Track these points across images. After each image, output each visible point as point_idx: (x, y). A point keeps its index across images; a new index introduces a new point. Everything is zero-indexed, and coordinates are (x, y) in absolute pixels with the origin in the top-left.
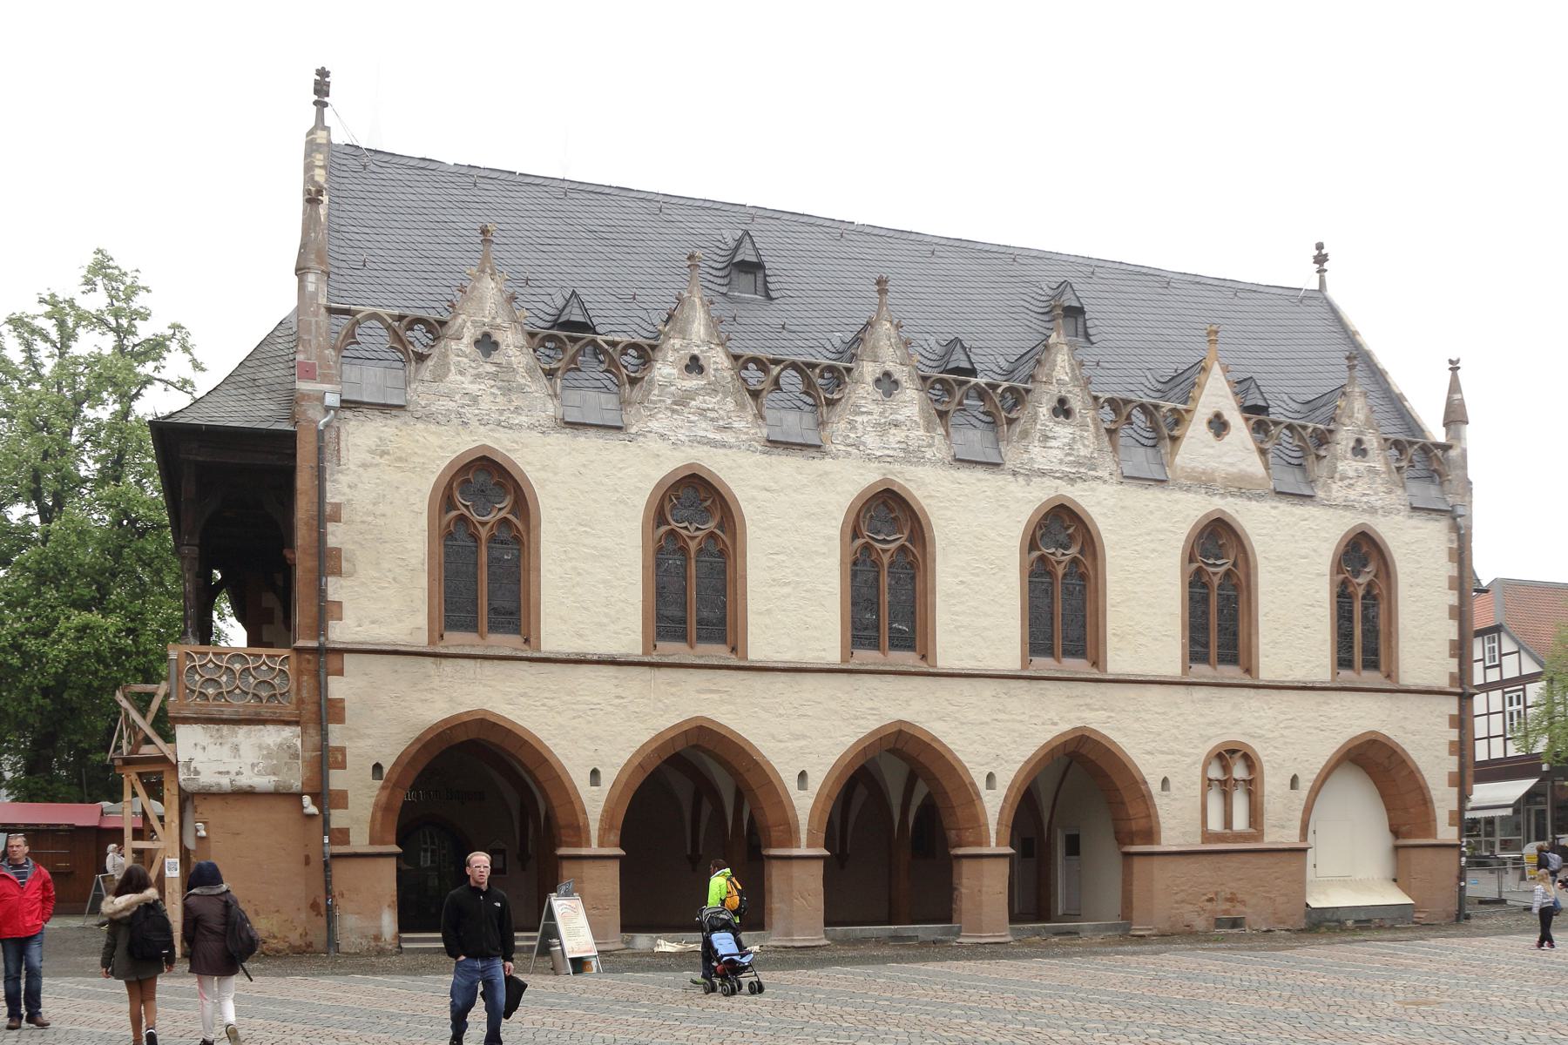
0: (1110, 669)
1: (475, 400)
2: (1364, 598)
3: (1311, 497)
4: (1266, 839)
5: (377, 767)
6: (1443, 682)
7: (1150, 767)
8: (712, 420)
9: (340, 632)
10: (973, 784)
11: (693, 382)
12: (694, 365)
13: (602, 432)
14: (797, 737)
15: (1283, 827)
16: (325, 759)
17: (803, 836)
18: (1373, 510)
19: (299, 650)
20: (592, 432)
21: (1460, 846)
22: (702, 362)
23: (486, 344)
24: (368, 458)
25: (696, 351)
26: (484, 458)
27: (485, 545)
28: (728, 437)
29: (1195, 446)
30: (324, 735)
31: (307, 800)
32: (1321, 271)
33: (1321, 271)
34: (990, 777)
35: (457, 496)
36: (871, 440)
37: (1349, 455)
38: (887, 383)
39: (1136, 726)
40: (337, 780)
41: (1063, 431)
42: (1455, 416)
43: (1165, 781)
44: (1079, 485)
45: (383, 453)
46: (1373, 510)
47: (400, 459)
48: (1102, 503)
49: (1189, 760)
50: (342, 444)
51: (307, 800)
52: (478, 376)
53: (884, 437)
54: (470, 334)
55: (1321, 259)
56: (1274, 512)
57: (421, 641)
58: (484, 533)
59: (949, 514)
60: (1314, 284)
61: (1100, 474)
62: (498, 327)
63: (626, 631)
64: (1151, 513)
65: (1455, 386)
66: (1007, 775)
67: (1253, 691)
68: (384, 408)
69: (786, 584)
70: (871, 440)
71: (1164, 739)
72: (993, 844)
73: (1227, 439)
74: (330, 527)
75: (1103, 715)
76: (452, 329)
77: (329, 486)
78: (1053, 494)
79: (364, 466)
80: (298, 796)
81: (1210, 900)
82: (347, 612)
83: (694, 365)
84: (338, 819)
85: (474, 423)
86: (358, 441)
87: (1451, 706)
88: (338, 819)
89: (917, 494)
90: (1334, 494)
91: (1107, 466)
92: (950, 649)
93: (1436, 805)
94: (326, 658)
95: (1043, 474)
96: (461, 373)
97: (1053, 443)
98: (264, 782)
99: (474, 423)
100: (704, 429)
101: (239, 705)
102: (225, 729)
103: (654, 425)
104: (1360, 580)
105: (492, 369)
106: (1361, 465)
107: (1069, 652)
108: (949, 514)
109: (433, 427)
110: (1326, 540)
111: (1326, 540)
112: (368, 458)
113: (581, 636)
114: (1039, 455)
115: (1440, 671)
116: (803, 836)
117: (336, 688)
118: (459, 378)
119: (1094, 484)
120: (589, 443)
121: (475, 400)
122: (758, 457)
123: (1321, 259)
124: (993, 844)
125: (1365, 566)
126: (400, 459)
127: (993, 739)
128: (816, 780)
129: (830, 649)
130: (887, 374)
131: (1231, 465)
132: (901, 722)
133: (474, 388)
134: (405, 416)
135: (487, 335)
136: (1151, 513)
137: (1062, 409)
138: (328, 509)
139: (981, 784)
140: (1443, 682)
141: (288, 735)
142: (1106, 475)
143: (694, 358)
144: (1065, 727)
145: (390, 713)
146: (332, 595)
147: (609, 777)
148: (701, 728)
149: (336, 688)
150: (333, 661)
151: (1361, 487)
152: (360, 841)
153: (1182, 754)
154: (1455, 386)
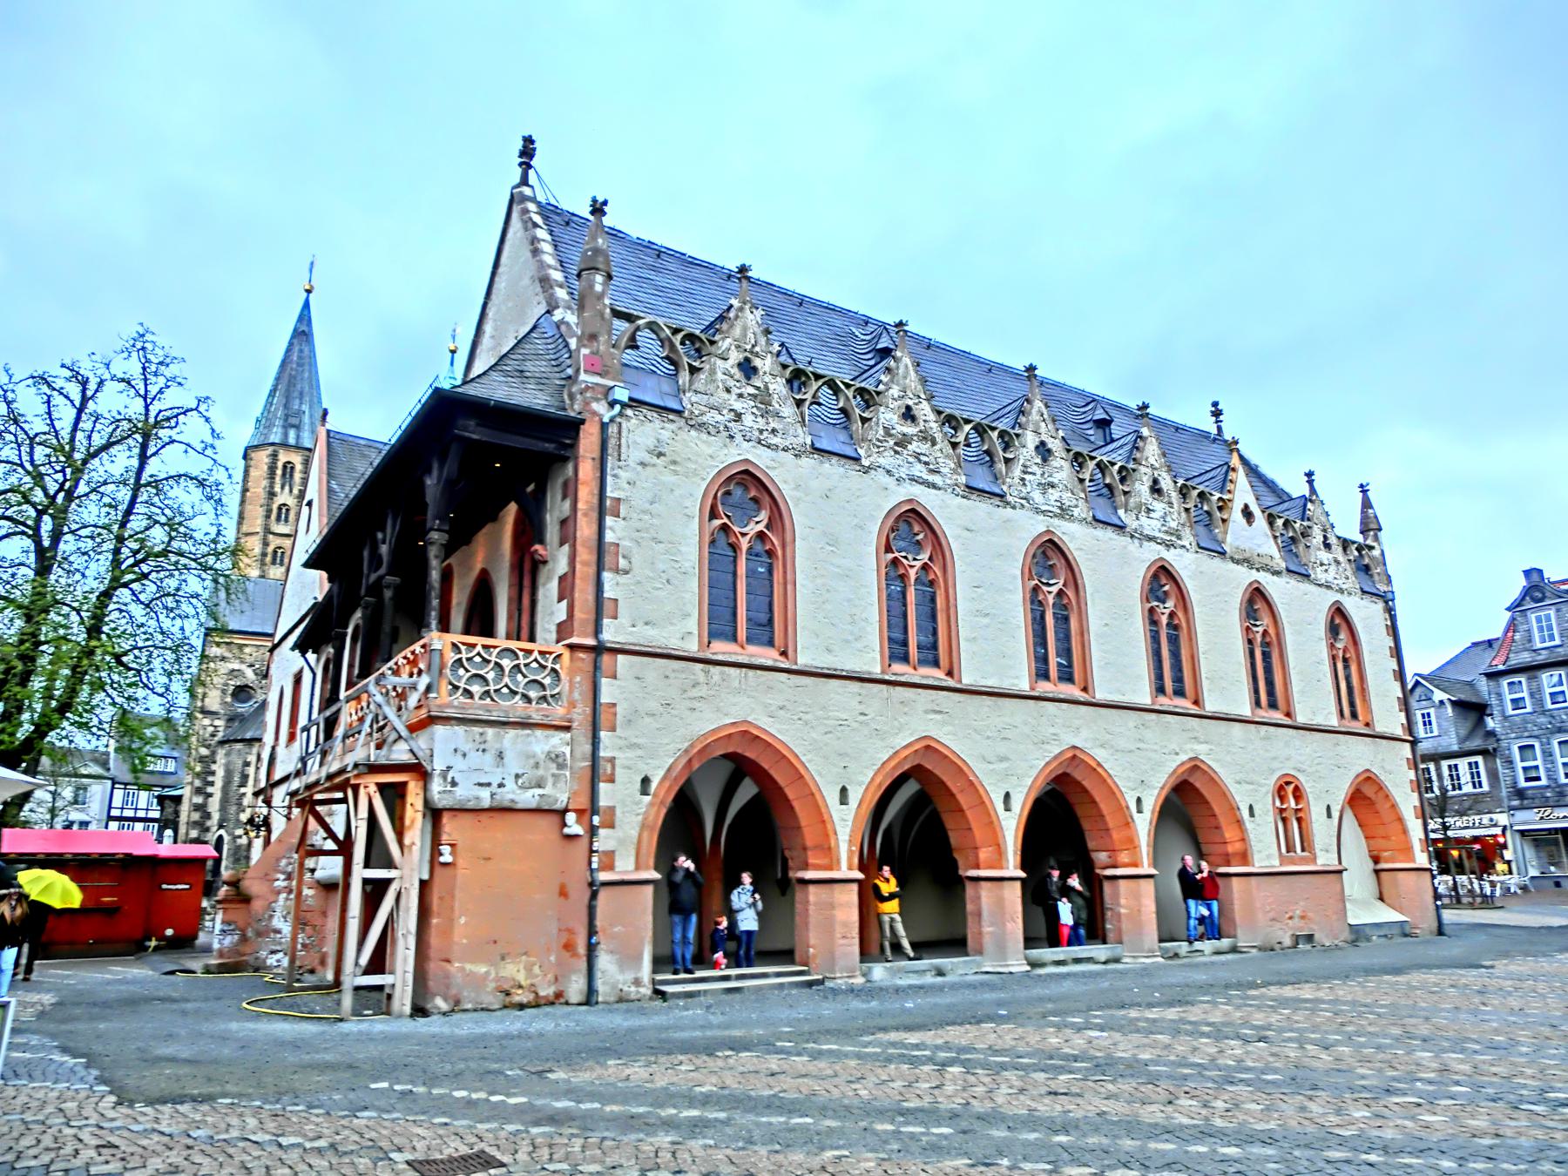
1: (738, 417)
8: (926, 463)
11: (910, 429)
13: (843, 461)
20: (835, 460)
22: (915, 412)
24: (647, 458)
25: (910, 403)
35: (720, 508)
36: (1037, 496)
42: (1370, 525)
45: (660, 455)
47: (674, 462)
50: (623, 441)
52: (740, 396)
53: (1045, 496)
54: (735, 357)
62: (757, 355)
65: (1367, 504)
70: (1037, 496)
79: (643, 464)
83: (909, 415)
85: (739, 437)
86: (639, 440)
89: (1071, 546)
95: (1151, 539)
96: (728, 391)
99: (739, 437)
100: (919, 470)
105: (752, 391)
109: (704, 436)
112: (647, 458)
118: (726, 396)
120: (833, 468)
121: (738, 417)
122: (959, 499)
126: (674, 462)
143: (908, 408)
154: (1367, 504)
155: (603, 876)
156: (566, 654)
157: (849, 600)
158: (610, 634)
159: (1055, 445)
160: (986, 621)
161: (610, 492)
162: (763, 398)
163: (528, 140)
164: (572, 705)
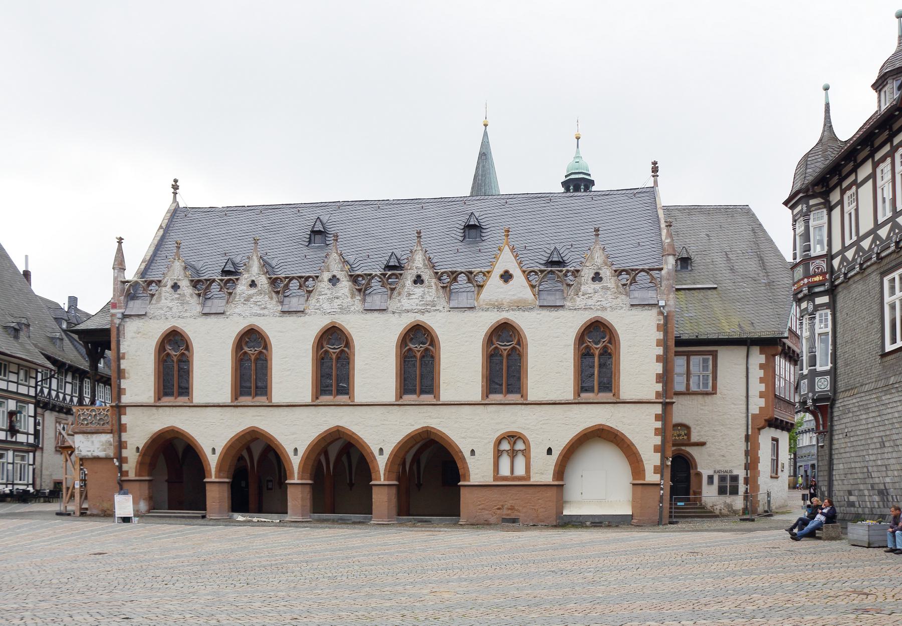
0: (441, 399)
1: (171, 309)
2: (601, 355)
3: (562, 306)
5: (138, 448)
6: (652, 397)
10: (372, 453)
11: (253, 291)
12: (253, 284)
15: (542, 474)
16: (121, 445)
17: (296, 475)
18: (604, 309)
20: (212, 316)
21: (659, 485)
23: (175, 287)
26: (174, 331)
27: (174, 367)
28: (265, 312)
29: (494, 288)
30: (120, 437)
34: (381, 450)
36: (326, 306)
37: (590, 281)
38: (334, 280)
40: (125, 453)
41: (419, 290)
43: (473, 452)
44: (427, 314)
46: (604, 309)
48: (439, 322)
49: (486, 441)
53: (333, 304)
54: (170, 284)
57: (151, 401)
58: (175, 359)
61: (437, 308)
63: (225, 394)
66: (388, 450)
67: (523, 406)
68: (139, 316)
70: (326, 306)
71: (471, 430)
73: (511, 283)
74: (122, 361)
76: (164, 282)
77: (121, 347)
79: (133, 338)
81: (499, 509)
83: (253, 284)
85: (170, 318)
87: (658, 409)
88: (125, 467)
90: (578, 303)
91: (442, 303)
93: (645, 463)
97: (413, 297)
98: (102, 454)
99: (170, 318)
100: (256, 310)
102: (89, 436)
103: (237, 310)
106: (597, 286)
107: (423, 392)
110: (571, 327)
111: (571, 327)
114: (406, 303)
115: (651, 388)
116: (296, 475)
117: (124, 420)
119: (434, 313)
120: (212, 320)
121: (171, 309)
122: (278, 318)
125: (603, 338)
127: (383, 432)
128: (301, 452)
129: (307, 396)
130: (334, 276)
131: (514, 295)
133: (170, 305)
134: (146, 318)
135: (176, 284)
137: (418, 280)
139: (376, 452)
140: (652, 397)
141: (108, 437)
142: (441, 308)
145: (141, 429)
146: (122, 386)
147: (219, 451)
149: (124, 420)
150: (122, 410)
151: (596, 297)
152: (132, 476)
159: (339, 275)
161: (122, 351)
162: (182, 300)
164: (113, 425)
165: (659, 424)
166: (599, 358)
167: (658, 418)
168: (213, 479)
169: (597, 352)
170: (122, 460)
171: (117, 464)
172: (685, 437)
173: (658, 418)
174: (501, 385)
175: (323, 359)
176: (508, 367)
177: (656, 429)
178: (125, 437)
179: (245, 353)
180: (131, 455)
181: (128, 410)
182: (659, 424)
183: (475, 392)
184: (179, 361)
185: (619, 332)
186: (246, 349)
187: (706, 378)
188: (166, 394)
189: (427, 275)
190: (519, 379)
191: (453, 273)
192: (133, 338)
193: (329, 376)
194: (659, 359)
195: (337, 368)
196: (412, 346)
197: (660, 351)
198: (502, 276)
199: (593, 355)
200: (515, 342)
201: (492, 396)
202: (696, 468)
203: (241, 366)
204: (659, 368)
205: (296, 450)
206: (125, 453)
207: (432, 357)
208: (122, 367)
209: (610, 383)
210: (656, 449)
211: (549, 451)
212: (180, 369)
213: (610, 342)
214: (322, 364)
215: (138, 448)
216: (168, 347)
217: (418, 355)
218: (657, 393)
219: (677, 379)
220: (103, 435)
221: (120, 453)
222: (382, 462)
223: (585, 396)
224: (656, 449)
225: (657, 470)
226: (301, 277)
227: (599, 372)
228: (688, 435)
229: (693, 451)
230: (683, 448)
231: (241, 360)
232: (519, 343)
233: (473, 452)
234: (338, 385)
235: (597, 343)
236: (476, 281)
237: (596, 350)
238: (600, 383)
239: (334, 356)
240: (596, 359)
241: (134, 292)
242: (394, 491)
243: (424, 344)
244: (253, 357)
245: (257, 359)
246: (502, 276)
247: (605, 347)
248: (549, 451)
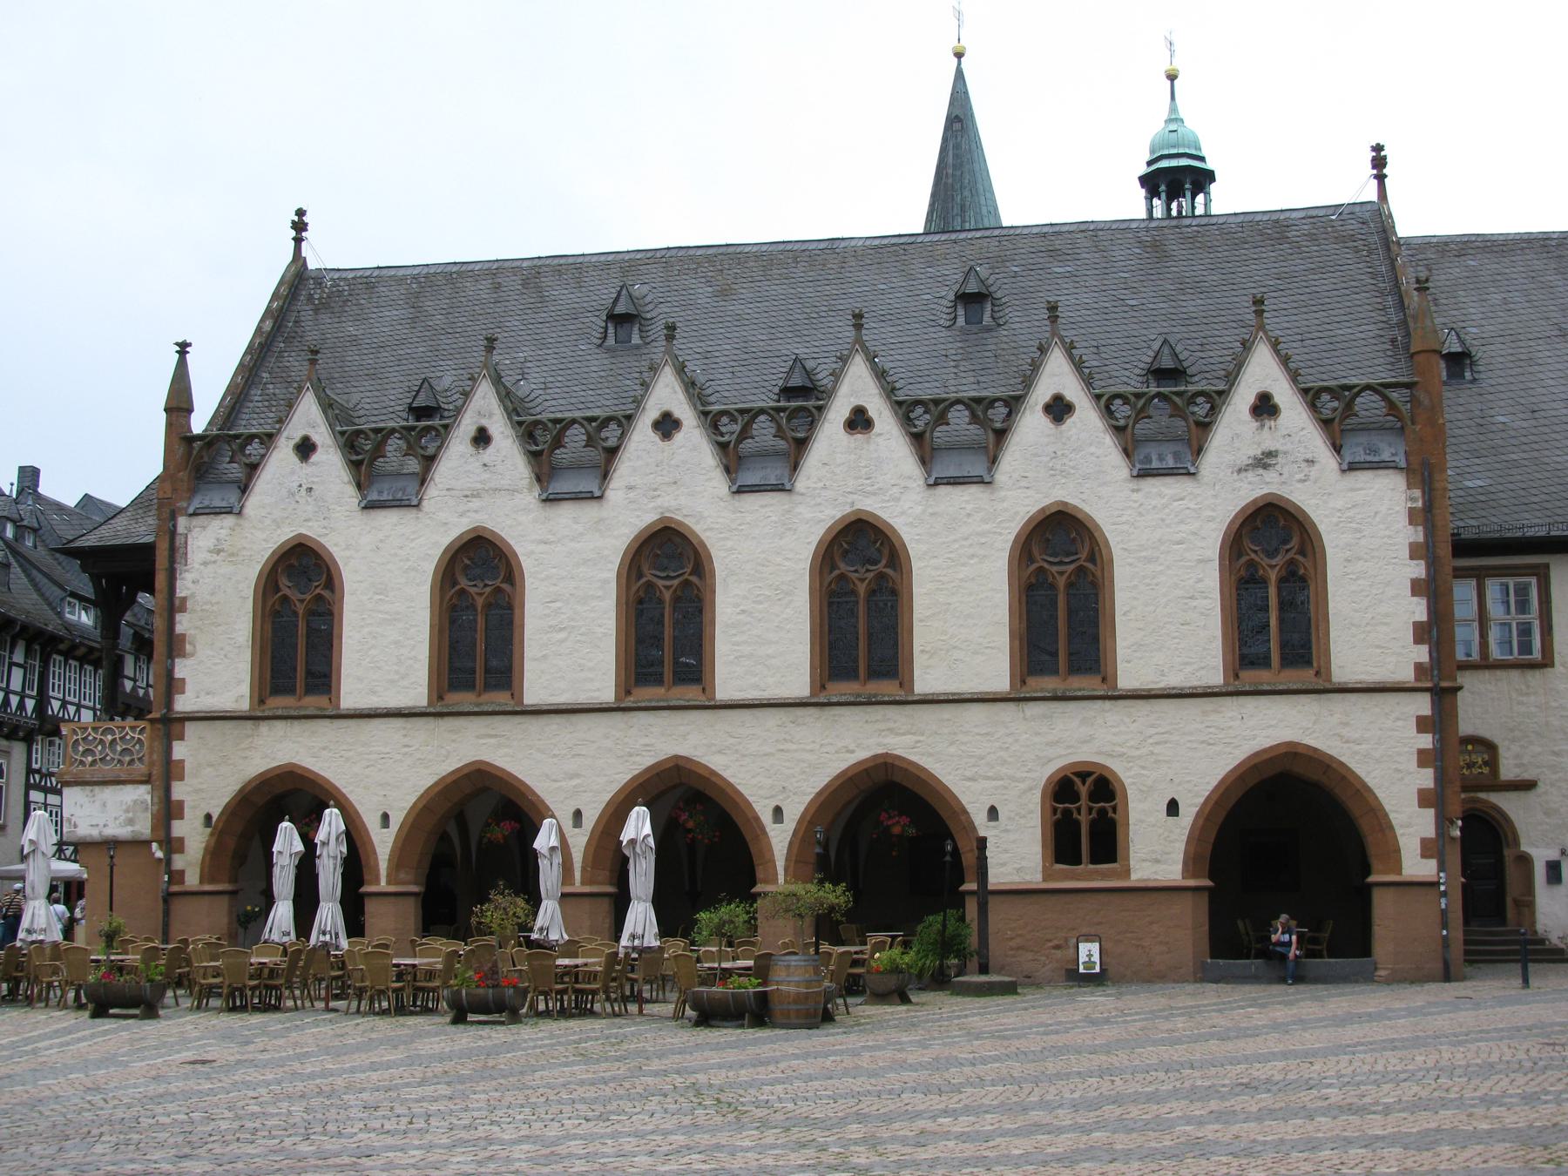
2: (1282, 581)
4: (1134, 877)
5: (208, 817)
6: (1407, 675)
7: (972, 797)
9: (183, 704)
10: (757, 819)
14: (572, 776)
15: (1157, 861)
16: (169, 810)
19: (152, 721)
21: (1438, 884)
24: (209, 557)
26: (300, 545)
30: (168, 790)
31: (154, 845)
32: (1381, 178)
33: (1381, 178)
39: (952, 750)
40: (179, 828)
43: (993, 813)
45: (219, 552)
47: (232, 555)
49: (1022, 786)
51: (154, 845)
55: (1379, 162)
56: (1135, 496)
59: (729, 544)
60: (1371, 194)
64: (969, 515)
66: (794, 811)
69: (562, 630)
72: (781, 879)
73: (1069, 421)
74: (178, 617)
75: (909, 739)
77: (178, 584)
78: (848, 510)
79: (205, 564)
80: (148, 843)
81: (1057, 947)
82: (188, 687)
84: (179, 862)
86: (201, 544)
87: (1422, 705)
88: (179, 862)
89: (697, 528)
92: (729, 679)
93: (1399, 831)
94: (171, 725)
101: (107, 770)
102: (97, 789)
104: (1274, 562)
108: (729, 544)
110: (1211, 519)
111: (1211, 519)
112: (209, 557)
113: (374, 693)
115: (1403, 657)
117: (179, 751)
123: (1379, 162)
124: (781, 879)
125: (1285, 542)
126: (232, 555)
132: (677, 757)
136: (969, 515)
138: (177, 603)
139: (766, 817)
140: (1407, 675)
141: (142, 793)
144: (862, 755)
146: (178, 674)
148: (479, 771)
149: (179, 751)
150: (176, 727)
152: (192, 880)
153: (1013, 779)
155: (175, 888)
156: (148, 727)
157: (396, 643)
158: (183, 704)
160: (562, 635)
161: (180, 593)
163: (301, 213)
164: (152, 764)
165: (1426, 741)
166: (1279, 589)
167: (1423, 725)
168: (383, 885)
169: (1273, 576)
170: (173, 846)
171: (159, 854)
172: (1486, 770)
173: (1423, 725)
174: (1055, 654)
175: (641, 602)
176: (1071, 612)
177: (1421, 752)
178: (179, 791)
179: (463, 592)
180: (192, 833)
181: (191, 729)
182: (1426, 741)
183: (996, 673)
184: (311, 613)
185: (1322, 528)
186: (464, 582)
187: (1525, 631)
188: (277, 690)
189: (879, 410)
190: (1096, 639)
191: (936, 402)
192: (205, 564)
193: (657, 641)
194: (1417, 587)
195: (676, 623)
196: (843, 567)
197: (1418, 569)
198: (1048, 409)
199: (1264, 582)
200: (1084, 555)
201: (1033, 682)
202: (1517, 842)
203: (453, 622)
204: (1418, 610)
205: (578, 815)
206: (179, 828)
207: (894, 592)
208: (179, 629)
209: (1307, 645)
210: (1424, 799)
211: (1173, 808)
212: (311, 632)
213: (1302, 552)
214: (640, 614)
215: (208, 817)
216: (284, 582)
217: (862, 589)
218: (1419, 667)
219: (1460, 633)
220: (129, 788)
221: (168, 828)
222: (779, 838)
223: (1250, 677)
224: (1424, 799)
225: (1428, 849)
226: (591, 420)
227: (1281, 621)
228: (1493, 763)
229: (1507, 803)
230: (1482, 795)
231: (453, 608)
232: (1092, 558)
233: (993, 813)
234: (676, 663)
235: (1271, 554)
236: (993, 422)
237: (1272, 569)
238: (1283, 645)
239: (667, 595)
240: (1272, 591)
241: (208, 461)
242: (1204, 901)
243: (875, 563)
244: (480, 601)
245: (488, 606)
246: (1048, 409)
247: (1292, 562)
248: (1173, 808)
